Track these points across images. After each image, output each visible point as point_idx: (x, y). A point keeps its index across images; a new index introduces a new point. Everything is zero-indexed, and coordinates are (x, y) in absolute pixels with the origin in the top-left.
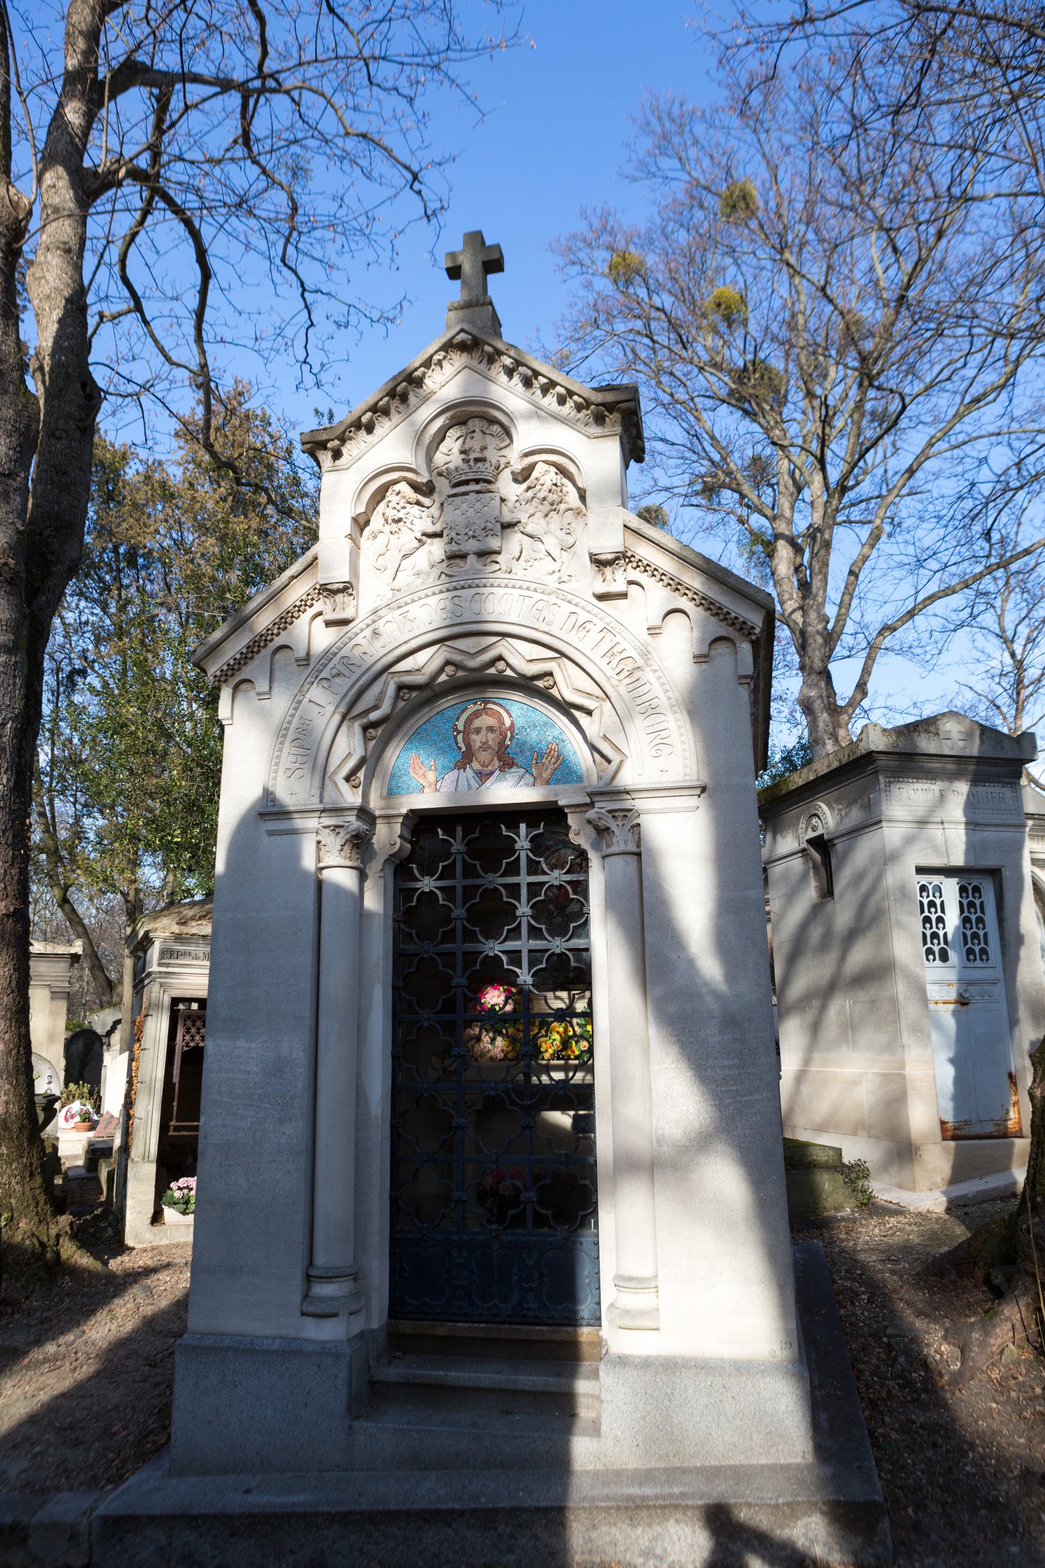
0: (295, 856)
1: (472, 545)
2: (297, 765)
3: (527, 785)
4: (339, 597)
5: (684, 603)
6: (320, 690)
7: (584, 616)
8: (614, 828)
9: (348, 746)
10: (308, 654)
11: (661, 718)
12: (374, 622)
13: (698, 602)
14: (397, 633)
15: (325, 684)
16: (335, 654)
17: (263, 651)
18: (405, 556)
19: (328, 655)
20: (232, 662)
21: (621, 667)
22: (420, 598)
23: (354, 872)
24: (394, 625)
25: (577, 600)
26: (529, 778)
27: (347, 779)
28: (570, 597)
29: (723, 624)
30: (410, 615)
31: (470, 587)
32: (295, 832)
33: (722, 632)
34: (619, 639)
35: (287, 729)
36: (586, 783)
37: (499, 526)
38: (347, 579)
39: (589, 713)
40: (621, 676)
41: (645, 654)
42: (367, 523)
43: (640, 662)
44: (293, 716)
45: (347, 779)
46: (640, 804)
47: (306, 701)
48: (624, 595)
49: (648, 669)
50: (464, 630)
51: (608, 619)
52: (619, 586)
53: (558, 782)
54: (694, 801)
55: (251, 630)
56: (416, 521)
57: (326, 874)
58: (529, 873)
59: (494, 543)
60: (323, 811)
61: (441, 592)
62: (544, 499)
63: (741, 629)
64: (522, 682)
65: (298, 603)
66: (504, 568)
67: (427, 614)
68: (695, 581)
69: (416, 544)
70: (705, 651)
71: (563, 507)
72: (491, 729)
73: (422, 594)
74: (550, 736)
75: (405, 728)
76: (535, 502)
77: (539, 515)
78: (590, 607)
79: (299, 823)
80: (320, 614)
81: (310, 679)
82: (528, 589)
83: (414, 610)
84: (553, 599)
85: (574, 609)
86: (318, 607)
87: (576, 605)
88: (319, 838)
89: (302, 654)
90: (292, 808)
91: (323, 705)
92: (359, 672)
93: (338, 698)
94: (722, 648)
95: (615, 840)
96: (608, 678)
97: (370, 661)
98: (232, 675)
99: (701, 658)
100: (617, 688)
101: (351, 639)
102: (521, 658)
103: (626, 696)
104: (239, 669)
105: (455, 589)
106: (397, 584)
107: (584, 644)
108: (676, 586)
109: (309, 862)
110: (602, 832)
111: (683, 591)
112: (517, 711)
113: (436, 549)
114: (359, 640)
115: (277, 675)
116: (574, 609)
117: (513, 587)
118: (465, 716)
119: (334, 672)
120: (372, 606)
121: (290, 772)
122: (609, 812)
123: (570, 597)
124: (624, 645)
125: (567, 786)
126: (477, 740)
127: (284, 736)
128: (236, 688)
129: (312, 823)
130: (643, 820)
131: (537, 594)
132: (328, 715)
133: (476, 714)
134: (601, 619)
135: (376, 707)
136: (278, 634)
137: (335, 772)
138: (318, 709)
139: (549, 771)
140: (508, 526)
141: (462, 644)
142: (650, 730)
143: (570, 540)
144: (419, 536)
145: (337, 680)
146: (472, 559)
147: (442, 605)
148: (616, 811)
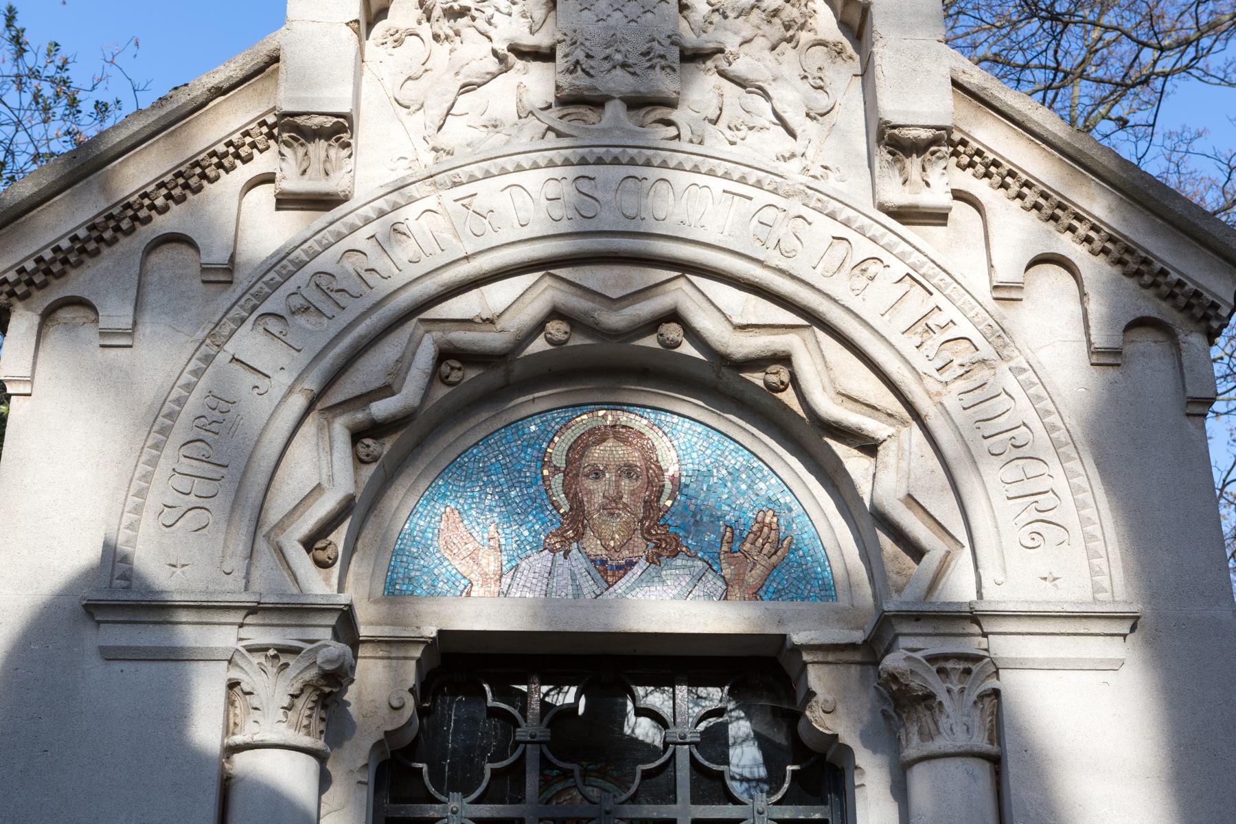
0: (176, 713)
1: (619, 82)
2: (193, 500)
3: (709, 596)
4: (318, 148)
5: (1067, 245)
6: (260, 338)
7: (863, 248)
8: (942, 696)
9: (317, 470)
10: (233, 257)
11: (1033, 468)
12: (396, 207)
13: (1097, 245)
14: (448, 236)
15: (274, 326)
16: (301, 265)
17: (124, 241)
18: (467, 88)
19: (284, 264)
20: (48, 255)
21: (946, 355)
22: (503, 172)
23: (311, 763)
24: (440, 222)
25: (846, 213)
26: (713, 583)
27: (309, 544)
28: (833, 205)
29: (1149, 293)
30: (476, 203)
31: (616, 161)
32: (177, 656)
33: (1149, 307)
34: (938, 298)
35: (171, 416)
36: (843, 601)
37: (676, 52)
38: (345, 109)
39: (870, 447)
40: (947, 376)
41: (1000, 335)
42: (382, 13)
43: (986, 351)
44: (189, 387)
45: (309, 544)
46: (1003, 646)
47: (223, 358)
48: (939, 217)
49: (1003, 367)
50: (607, 247)
51: (916, 257)
52: (936, 196)
53: (778, 594)
54: (1115, 649)
55: (105, 189)
56: (498, 18)
57: (242, 763)
58: (696, 799)
59: (666, 84)
60: (252, 611)
61: (551, 164)
62: (776, 13)
63: (1189, 307)
64: (709, 375)
65: (221, 148)
66: (686, 134)
67: (525, 203)
68: (1097, 204)
69: (492, 65)
70: (1116, 342)
71: (805, 37)
72: (628, 470)
73: (509, 163)
74: (767, 487)
75: (432, 451)
76: (756, 16)
77: (760, 42)
78: (877, 230)
79: (190, 634)
80: (268, 179)
81: (237, 312)
82: (743, 180)
83: (488, 193)
84: (796, 207)
85: (842, 231)
86: (262, 163)
87: (846, 224)
88: (235, 674)
89: (219, 256)
90: (177, 598)
93: (304, 359)
94: (1146, 342)
95: (944, 722)
96: (919, 376)
98: (44, 285)
99: (1107, 358)
100: (943, 399)
101: (340, 237)
102: (724, 318)
103: (959, 416)
104: (62, 274)
105: (583, 162)
106: (443, 140)
107: (875, 302)
108: (1053, 210)
109: (206, 730)
110: (900, 705)
111: (1066, 220)
112: (682, 441)
113: (538, 83)
114: (359, 240)
115: (152, 297)
116: (842, 231)
117: (712, 173)
118: (570, 436)
119: (297, 302)
120: (392, 177)
121: (175, 513)
122: (932, 659)
124: (950, 312)
125: (798, 605)
126: (596, 492)
127: (165, 431)
128: (47, 316)
129: (224, 637)
130: (1009, 681)
131: (764, 187)
132: (277, 392)
133: (598, 435)
134: (901, 257)
135: (386, 391)
136: (164, 210)
137: (281, 526)
138: (253, 379)
139: (758, 570)
140: (694, 57)
141: (592, 277)
142: (1014, 490)
143: (822, 101)
144: (502, 48)
145: (301, 320)
146: (615, 110)
147: (553, 190)
148: (946, 657)
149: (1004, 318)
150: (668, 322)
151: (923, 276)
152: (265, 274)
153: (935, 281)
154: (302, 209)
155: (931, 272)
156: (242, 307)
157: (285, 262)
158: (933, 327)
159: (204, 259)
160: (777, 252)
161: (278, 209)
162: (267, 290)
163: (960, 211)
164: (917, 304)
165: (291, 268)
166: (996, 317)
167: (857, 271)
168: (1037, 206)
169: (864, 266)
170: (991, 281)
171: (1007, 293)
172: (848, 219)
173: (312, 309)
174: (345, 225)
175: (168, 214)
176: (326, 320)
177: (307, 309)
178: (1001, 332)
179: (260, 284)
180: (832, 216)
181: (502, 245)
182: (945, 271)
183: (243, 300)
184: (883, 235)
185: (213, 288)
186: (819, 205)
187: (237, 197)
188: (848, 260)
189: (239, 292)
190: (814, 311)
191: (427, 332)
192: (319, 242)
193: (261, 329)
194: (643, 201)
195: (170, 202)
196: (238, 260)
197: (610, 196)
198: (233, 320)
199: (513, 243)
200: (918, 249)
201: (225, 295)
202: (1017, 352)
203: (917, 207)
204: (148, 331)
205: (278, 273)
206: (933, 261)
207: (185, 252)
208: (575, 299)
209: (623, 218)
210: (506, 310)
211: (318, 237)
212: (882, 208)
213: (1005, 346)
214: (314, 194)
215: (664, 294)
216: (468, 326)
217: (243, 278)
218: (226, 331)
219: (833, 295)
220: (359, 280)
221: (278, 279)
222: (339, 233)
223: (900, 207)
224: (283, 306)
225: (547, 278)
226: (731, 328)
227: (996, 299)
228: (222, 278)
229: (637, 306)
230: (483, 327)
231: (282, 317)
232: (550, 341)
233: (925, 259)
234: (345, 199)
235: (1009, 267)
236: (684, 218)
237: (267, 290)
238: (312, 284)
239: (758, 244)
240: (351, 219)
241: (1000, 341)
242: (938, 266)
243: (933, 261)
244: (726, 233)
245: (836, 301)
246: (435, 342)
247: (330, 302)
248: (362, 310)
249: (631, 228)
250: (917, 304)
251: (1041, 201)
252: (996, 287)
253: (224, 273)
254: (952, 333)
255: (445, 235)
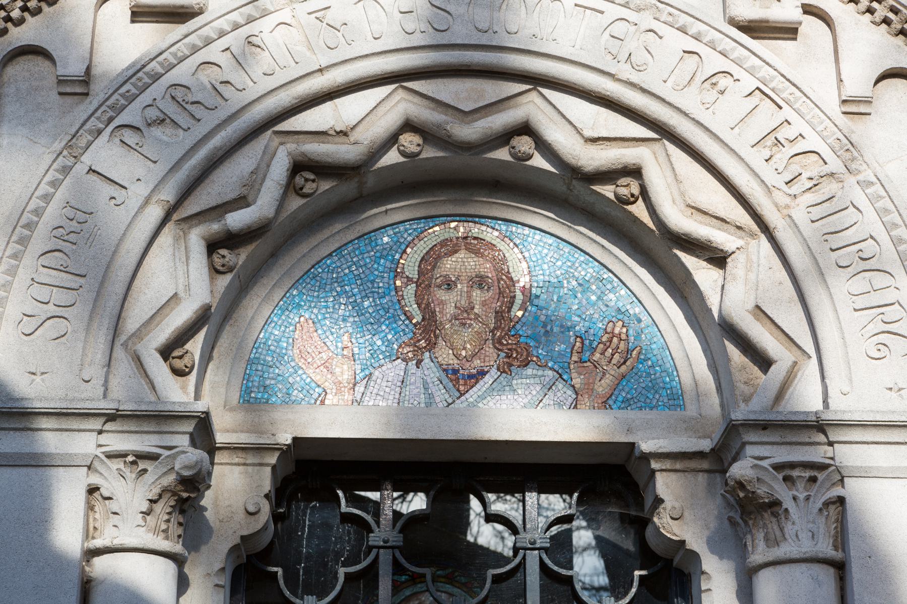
0: (39, 518)
2: (51, 309)
3: (559, 405)
6: (117, 149)
8: (788, 503)
9: (176, 278)
10: (88, 69)
11: (880, 280)
12: (250, 20)
15: (130, 137)
19: (140, 77)
21: (795, 169)
23: (170, 567)
24: (293, 36)
26: (564, 392)
27: (166, 352)
28: (683, 19)
32: (38, 462)
35: (29, 226)
36: (691, 410)
39: (719, 259)
40: (795, 189)
41: (850, 149)
43: (835, 164)
44: (47, 198)
45: (166, 352)
46: (848, 455)
47: (80, 169)
48: (789, 32)
49: (851, 180)
51: (766, 72)
53: (627, 403)
57: (101, 566)
60: (111, 417)
64: (560, 187)
72: (480, 281)
74: (617, 298)
75: (287, 261)
78: (727, 44)
79: (51, 440)
81: (93, 123)
84: (646, 20)
87: (697, 38)
88: (95, 480)
89: (75, 69)
90: (38, 405)
91: (131, 180)
92: (210, 120)
93: (160, 169)
95: (789, 529)
96: (768, 189)
97: (237, 100)
100: (792, 214)
101: (195, 50)
102: (575, 132)
107: (726, 118)
109: (67, 536)
110: (747, 511)
112: (536, 252)
114: (213, 53)
118: (422, 247)
119: (153, 113)
121: (33, 323)
122: (778, 467)
123: (683, 19)
124: (799, 126)
125: (647, 414)
126: (448, 303)
127: (24, 241)
129: (84, 443)
130: (853, 489)
132: (134, 203)
133: (450, 247)
134: (751, 71)
135: (241, 202)
136: (20, 22)
137: (138, 335)
138: (112, 190)
139: (608, 380)
142: (861, 302)
145: (157, 132)
148: (792, 465)
149: (853, 132)
150: (519, 135)
151: (773, 90)
152: (121, 86)
153: (785, 95)
154: (157, 22)
155: (780, 86)
156: (98, 118)
157: (140, 74)
158: (782, 141)
159: (61, 71)
160: (628, 66)
161: (133, 21)
162: (123, 102)
163: (811, 26)
164: (766, 117)
165: (147, 80)
166: (845, 131)
167: (707, 85)
168: (886, 21)
169: (714, 80)
170: (840, 95)
171: (855, 107)
172: (699, 33)
173: (168, 121)
174: (200, 37)
175: (23, 26)
176: (181, 132)
177: (163, 120)
178: (849, 146)
179: (116, 96)
180: (683, 30)
181: (356, 58)
182: (794, 85)
183: (100, 112)
184: (733, 49)
185: (69, 100)
186: (670, 19)
187: (92, 10)
188: (698, 74)
189: (95, 104)
190: (665, 124)
191: (282, 144)
192: (174, 55)
193: (117, 140)
194: (496, 15)
195: (26, 14)
196: (94, 71)
197: (462, 10)
198: (90, 132)
199: (367, 56)
200: (768, 64)
201: (82, 107)
202: (865, 166)
203: (767, 21)
204: (5, 142)
205: (134, 85)
206: (782, 75)
207: (41, 64)
208: (428, 111)
209: (475, 32)
210: (360, 122)
211: (173, 49)
212: (733, 22)
213: (853, 159)
214: (168, 7)
215: (516, 106)
216: (322, 138)
217: (99, 90)
218: (83, 142)
219: (684, 108)
220: (214, 93)
221: (134, 91)
222: (194, 46)
223: (750, 21)
224: (139, 118)
225: (400, 91)
226: (582, 141)
227: (844, 113)
228: (78, 90)
229: (490, 119)
230: (337, 139)
231: (138, 129)
232: (403, 153)
233: (776, 73)
234: (200, 12)
235: (858, 83)
236: (536, 31)
237: (123, 102)
238: (168, 96)
239: (610, 57)
240: (205, 31)
241: (848, 155)
242: (788, 80)
243: (782, 75)
244: (577, 47)
245: (686, 115)
246: (289, 154)
247: (185, 114)
248: (217, 122)
249: (484, 41)
250: (766, 117)
251: (891, 15)
252: (844, 102)
253: (79, 86)
254: (801, 146)
255: (299, 48)
